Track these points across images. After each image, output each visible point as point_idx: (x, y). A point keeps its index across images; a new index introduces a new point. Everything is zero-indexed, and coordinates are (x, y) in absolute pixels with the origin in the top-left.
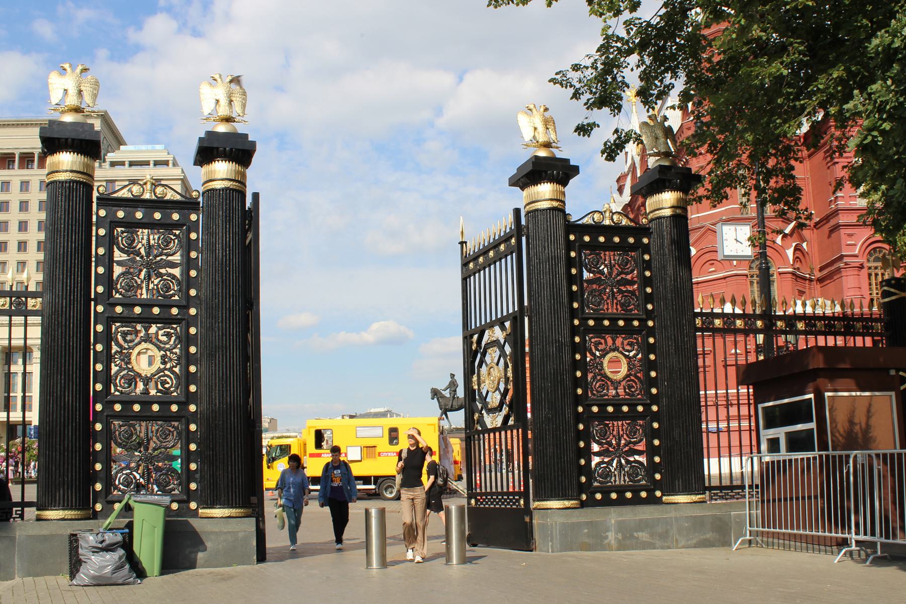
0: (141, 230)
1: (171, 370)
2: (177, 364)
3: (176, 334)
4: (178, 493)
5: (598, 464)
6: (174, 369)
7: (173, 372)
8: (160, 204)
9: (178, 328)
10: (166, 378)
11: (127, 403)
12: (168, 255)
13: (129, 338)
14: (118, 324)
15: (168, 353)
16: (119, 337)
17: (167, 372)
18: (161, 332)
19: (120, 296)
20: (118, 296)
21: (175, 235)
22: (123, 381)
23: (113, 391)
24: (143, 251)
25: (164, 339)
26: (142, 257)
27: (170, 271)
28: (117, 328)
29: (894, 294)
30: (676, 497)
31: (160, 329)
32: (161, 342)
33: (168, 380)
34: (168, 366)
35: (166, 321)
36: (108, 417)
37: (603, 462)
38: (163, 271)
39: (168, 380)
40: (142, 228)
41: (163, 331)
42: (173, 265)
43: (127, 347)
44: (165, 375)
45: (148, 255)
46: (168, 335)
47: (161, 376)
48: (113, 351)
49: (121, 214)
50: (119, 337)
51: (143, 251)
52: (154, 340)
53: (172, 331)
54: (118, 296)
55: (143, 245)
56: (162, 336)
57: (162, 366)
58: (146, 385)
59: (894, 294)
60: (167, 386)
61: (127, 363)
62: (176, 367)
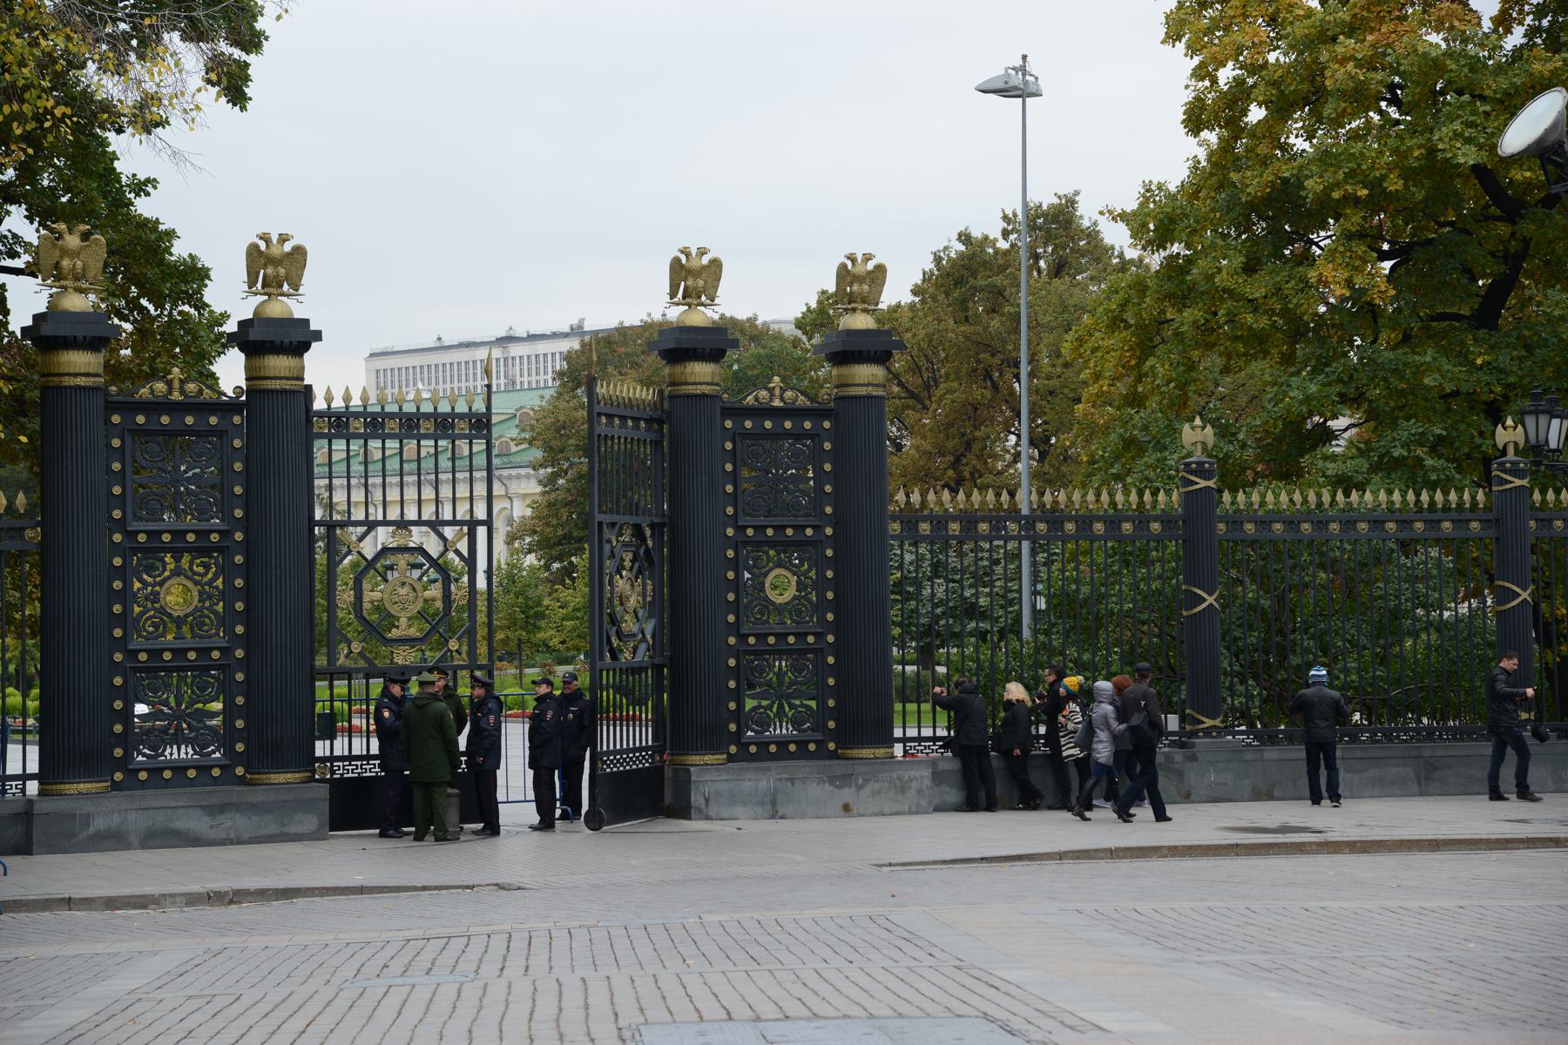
5: (754, 709)
7: (216, 613)
11: (155, 653)
15: (207, 588)
25: (201, 570)
29: (1511, 482)
30: (864, 751)
32: (195, 573)
36: (132, 669)
37: (760, 706)
41: (198, 561)
46: (207, 567)
48: (135, 589)
58: (179, 628)
59: (1511, 482)
60: (205, 628)
61: (154, 602)
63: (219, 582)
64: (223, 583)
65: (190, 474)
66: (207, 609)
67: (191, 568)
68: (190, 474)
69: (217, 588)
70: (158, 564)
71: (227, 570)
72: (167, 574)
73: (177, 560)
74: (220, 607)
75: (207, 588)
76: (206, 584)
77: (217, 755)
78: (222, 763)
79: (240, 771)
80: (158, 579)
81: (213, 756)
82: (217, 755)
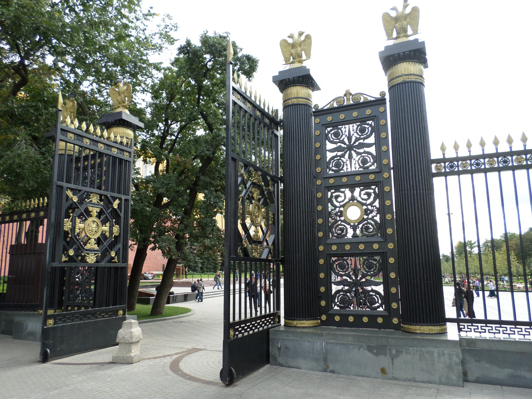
0: (344, 126)
1: (372, 219)
2: (377, 214)
3: (375, 192)
4: (383, 310)
6: (375, 218)
7: (375, 221)
8: (358, 106)
9: (377, 189)
10: (369, 225)
12: (364, 139)
13: (340, 199)
14: (333, 191)
15: (369, 207)
16: (334, 200)
17: (370, 221)
18: (363, 192)
19: (333, 172)
20: (331, 172)
21: (368, 124)
22: (338, 228)
23: (331, 237)
24: (346, 140)
25: (366, 197)
26: (345, 144)
27: (367, 149)
28: (332, 193)
31: (361, 190)
32: (363, 199)
33: (370, 226)
34: (370, 216)
35: (366, 185)
38: (361, 151)
39: (370, 226)
40: (345, 125)
42: (369, 145)
43: (339, 206)
44: (368, 223)
45: (350, 142)
46: (369, 195)
47: (365, 224)
49: (329, 118)
50: (334, 200)
51: (346, 140)
52: (359, 199)
53: (372, 191)
54: (331, 172)
55: (346, 136)
56: (364, 195)
57: (365, 217)
58: (355, 230)
61: (340, 216)
62: (376, 216)
63: (377, 204)
64: (379, 203)
65: (357, 143)
66: (370, 219)
67: (360, 196)
68: (357, 143)
69: (375, 206)
70: (342, 195)
71: (382, 196)
72: (347, 200)
73: (352, 191)
74: (378, 218)
75: (369, 207)
76: (369, 204)
77: (381, 309)
78: (383, 314)
79: (395, 321)
80: (342, 204)
81: (378, 309)
82: (381, 309)
